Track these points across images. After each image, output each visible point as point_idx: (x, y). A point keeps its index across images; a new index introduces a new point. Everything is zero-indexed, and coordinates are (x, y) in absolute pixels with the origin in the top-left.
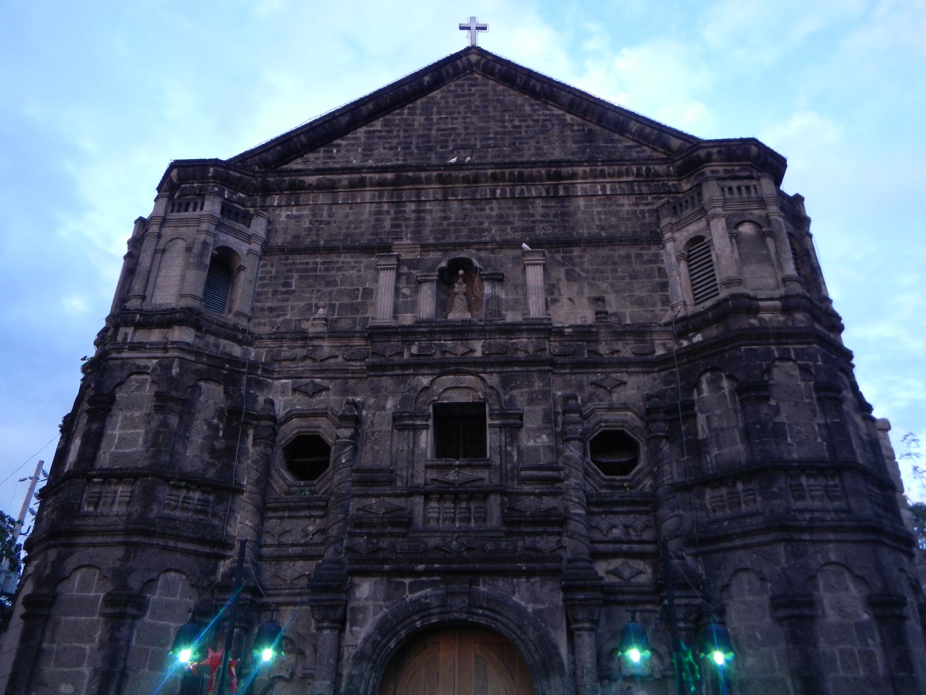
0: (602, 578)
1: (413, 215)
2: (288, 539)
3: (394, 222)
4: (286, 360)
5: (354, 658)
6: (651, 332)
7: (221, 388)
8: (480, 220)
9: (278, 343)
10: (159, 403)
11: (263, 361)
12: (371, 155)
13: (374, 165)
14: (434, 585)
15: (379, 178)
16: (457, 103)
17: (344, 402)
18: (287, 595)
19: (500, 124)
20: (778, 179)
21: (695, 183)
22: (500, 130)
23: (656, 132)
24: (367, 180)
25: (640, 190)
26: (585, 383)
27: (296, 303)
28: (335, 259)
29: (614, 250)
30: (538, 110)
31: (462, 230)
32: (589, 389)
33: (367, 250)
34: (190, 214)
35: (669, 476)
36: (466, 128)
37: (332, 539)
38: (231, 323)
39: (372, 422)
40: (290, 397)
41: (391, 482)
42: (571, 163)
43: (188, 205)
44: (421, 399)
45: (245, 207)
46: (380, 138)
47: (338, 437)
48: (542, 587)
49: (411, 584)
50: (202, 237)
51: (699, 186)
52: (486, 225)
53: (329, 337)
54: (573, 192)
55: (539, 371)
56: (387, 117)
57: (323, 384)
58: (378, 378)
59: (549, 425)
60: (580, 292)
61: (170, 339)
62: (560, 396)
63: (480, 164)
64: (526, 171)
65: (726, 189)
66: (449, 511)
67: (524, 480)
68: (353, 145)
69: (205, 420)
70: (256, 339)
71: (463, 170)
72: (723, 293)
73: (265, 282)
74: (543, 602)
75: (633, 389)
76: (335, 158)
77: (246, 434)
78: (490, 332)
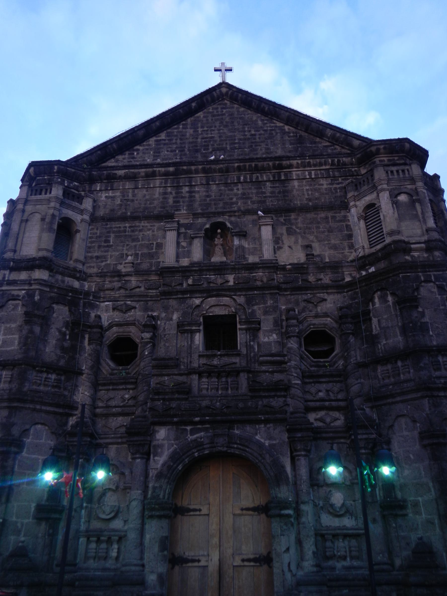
0: (312, 424)
1: (187, 195)
3: (175, 199)
4: (108, 290)
5: (156, 476)
6: (342, 266)
7: (67, 308)
8: (231, 197)
9: (102, 279)
10: (27, 319)
11: (93, 290)
12: (159, 156)
13: (161, 162)
14: (206, 430)
15: (165, 171)
16: (214, 120)
17: (146, 316)
19: (242, 133)
20: (423, 164)
21: (369, 169)
22: (242, 137)
23: (343, 136)
24: (157, 172)
25: (334, 174)
26: (300, 300)
27: (114, 253)
28: (137, 224)
29: (318, 214)
30: (267, 123)
31: (219, 203)
32: (303, 304)
33: (158, 218)
34: (43, 196)
35: (354, 358)
36: (220, 137)
37: (140, 403)
38: (72, 266)
39: (164, 328)
40: (112, 313)
41: (177, 366)
42: (288, 158)
43: (41, 190)
44: (195, 313)
45: (78, 191)
46: (165, 144)
47: (142, 338)
48: (274, 430)
49: (191, 430)
50: (51, 211)
51: (372, 171)
52: (234, 200)
53: (135, 274)
54: (291, 177)
55: (271, 294)
56: (169, 130)
57: (132, 305)
60: (296, 242)
61: (33, 278)
62: (284, 309)
63: (230, 160)
64: (260, 164)
65: (389, 172)
66: (215, 383)
67: (262, 363)
68: (147, 149)
69: (57, 329)
71: (218, 164)
72: (388, 240)
73: (93, 240)
75: (331, 304)
76: (136, 158)
77: (84, 338)
78: (239, 269)
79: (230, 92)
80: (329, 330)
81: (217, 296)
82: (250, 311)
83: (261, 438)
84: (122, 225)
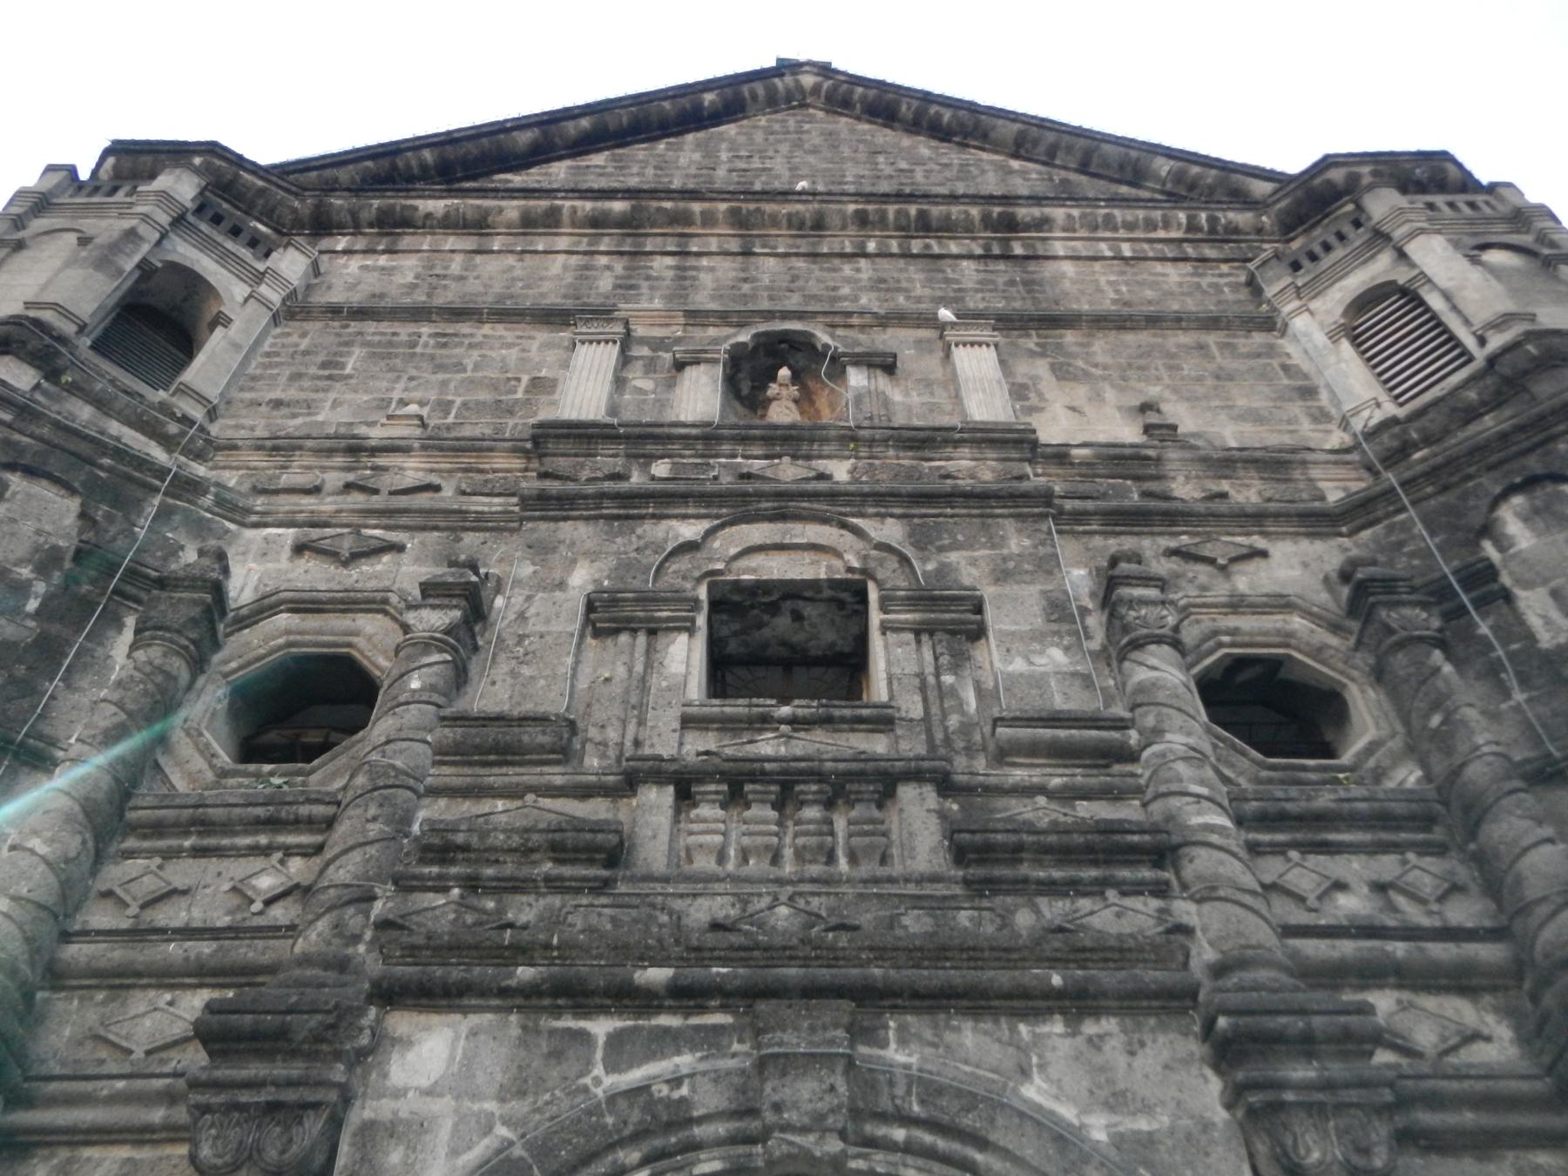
2: (173, 915)
6: (1304, 463)
7: (74, 504)
14: (711, 1039)
15: (593, 209)
18: (114, 1099)
23: (1214, 172)
24: (565, 211)
29: (1164, 337)
41: (563, 753)
48: (1132, 1053)
49: (615, 1040)
53: (424, 448)
58: (552, 525)
59: (1065, 627)
63: (830, 194)
64: (936, 211)
66: (763, 828)
70: (219, 448)
71: (787, 201)
74: (1147, 1109)
78: (871, 442)
79: (827, 84)
80: (1307, 654)
81: (780, 517)
82: (930, 567)
83: (1057, 1098)
84: (404, 331)
